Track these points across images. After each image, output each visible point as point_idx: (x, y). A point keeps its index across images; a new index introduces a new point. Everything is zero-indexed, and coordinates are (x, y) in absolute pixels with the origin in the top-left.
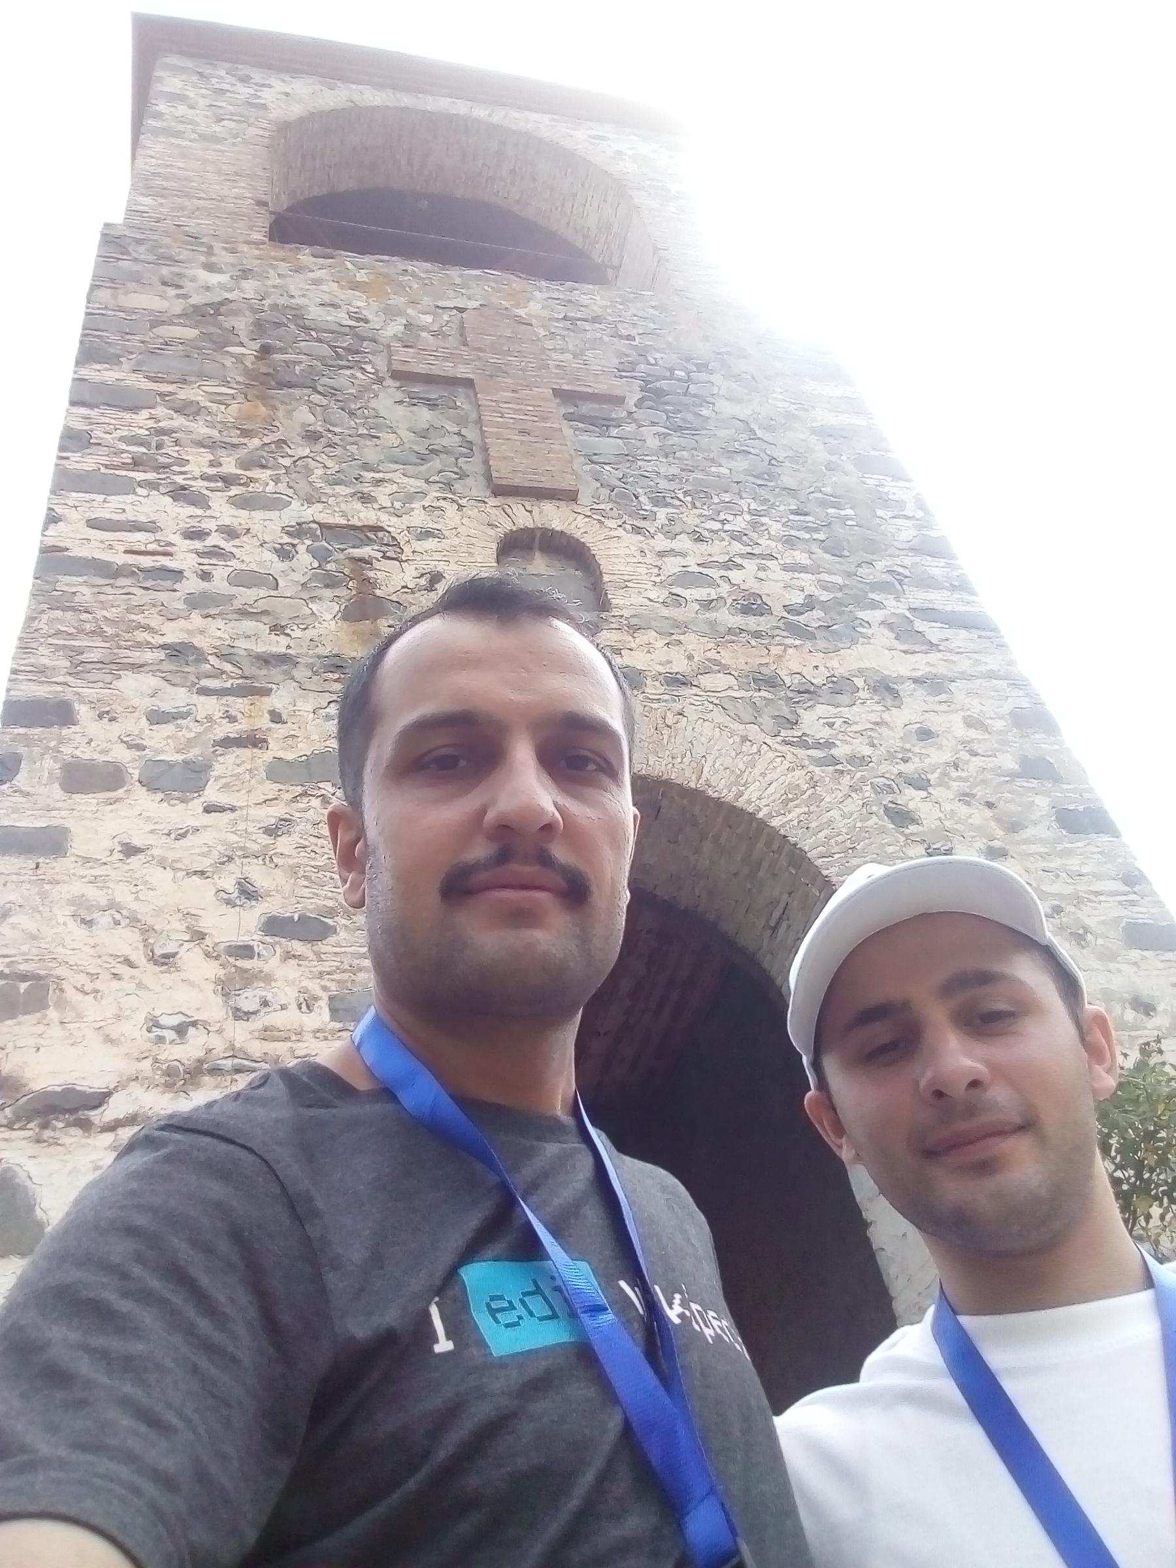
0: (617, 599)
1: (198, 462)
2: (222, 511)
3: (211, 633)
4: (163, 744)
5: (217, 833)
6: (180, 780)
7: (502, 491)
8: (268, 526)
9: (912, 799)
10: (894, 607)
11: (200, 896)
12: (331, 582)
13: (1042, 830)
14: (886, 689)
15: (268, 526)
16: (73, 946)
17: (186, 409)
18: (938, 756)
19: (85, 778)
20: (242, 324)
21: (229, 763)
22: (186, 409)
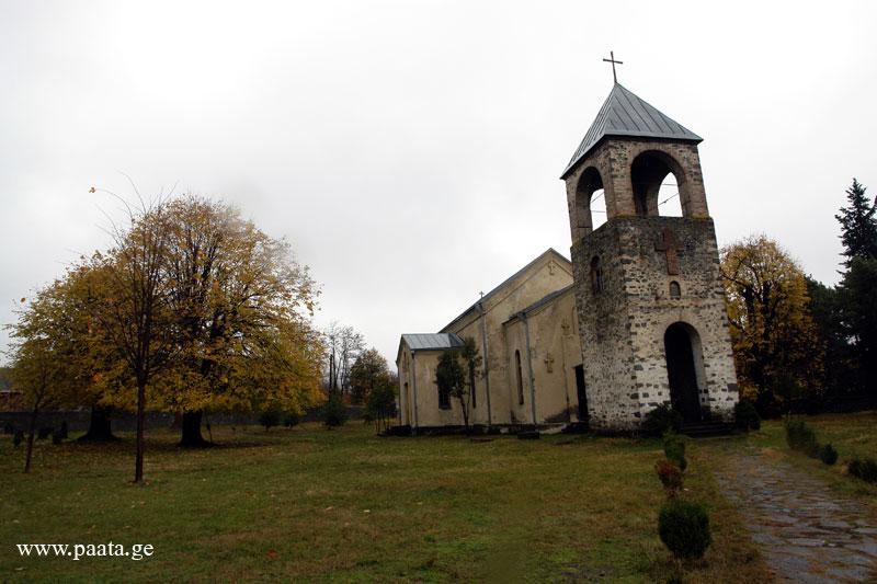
0: (683, 294)
1: (638, 274)
2: (642, 284)
3: (642, 304)
4: (642, 321)
5: (649, 332)
6: (644, 325)
7: (670, 274)
8: (646, 284)
9: (709, 324)
10: (712, 292)
11: (646, 339)
12: (653, 294)
13: (721, 327)
14: (709, 306)
15: (646, 284)
16: (641, 345)
17: (635, 263)
18: (712, 317)
19: (637, 326)
20: (637, 240)
21: (648, 323)
22: (635, 263)
